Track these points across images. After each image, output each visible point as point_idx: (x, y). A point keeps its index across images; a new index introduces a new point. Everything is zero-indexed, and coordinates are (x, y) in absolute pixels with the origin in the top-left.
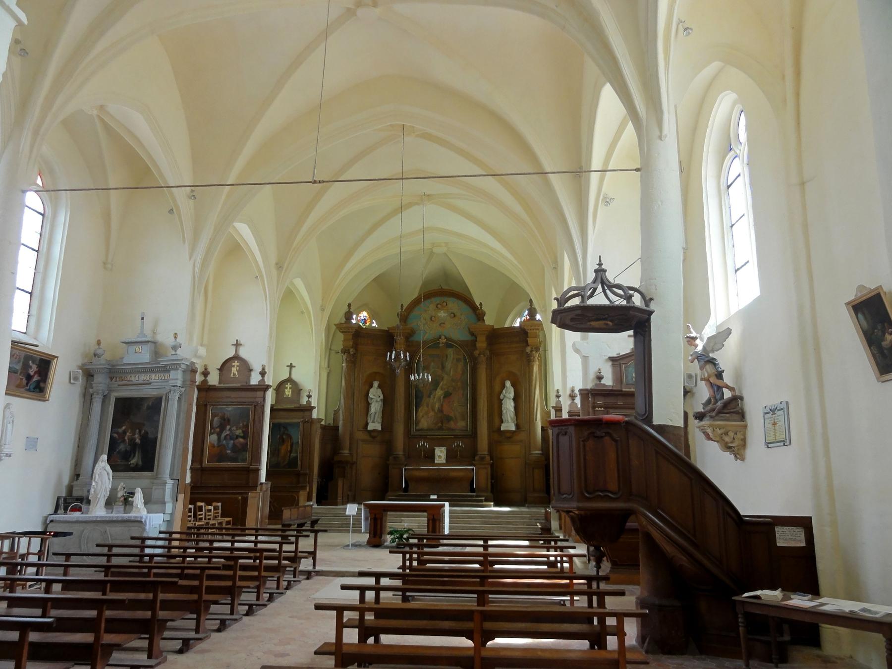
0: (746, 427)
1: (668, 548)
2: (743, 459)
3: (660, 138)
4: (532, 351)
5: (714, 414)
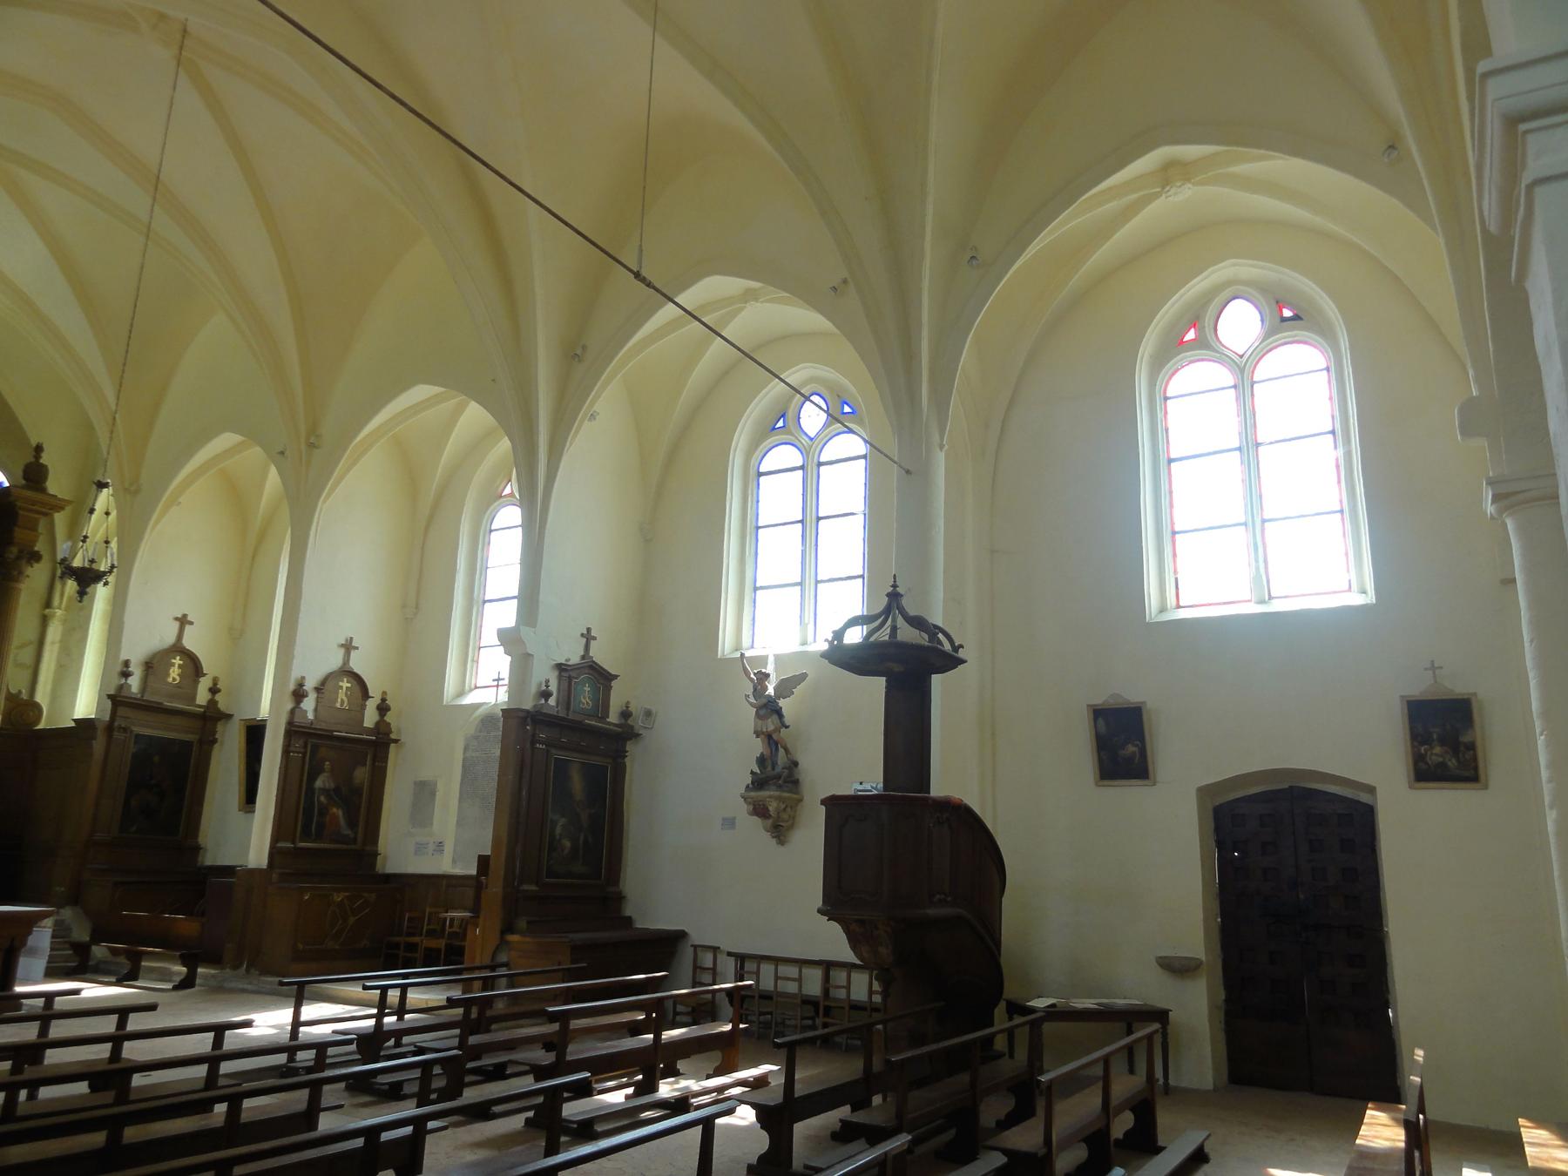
4: (18, 558)
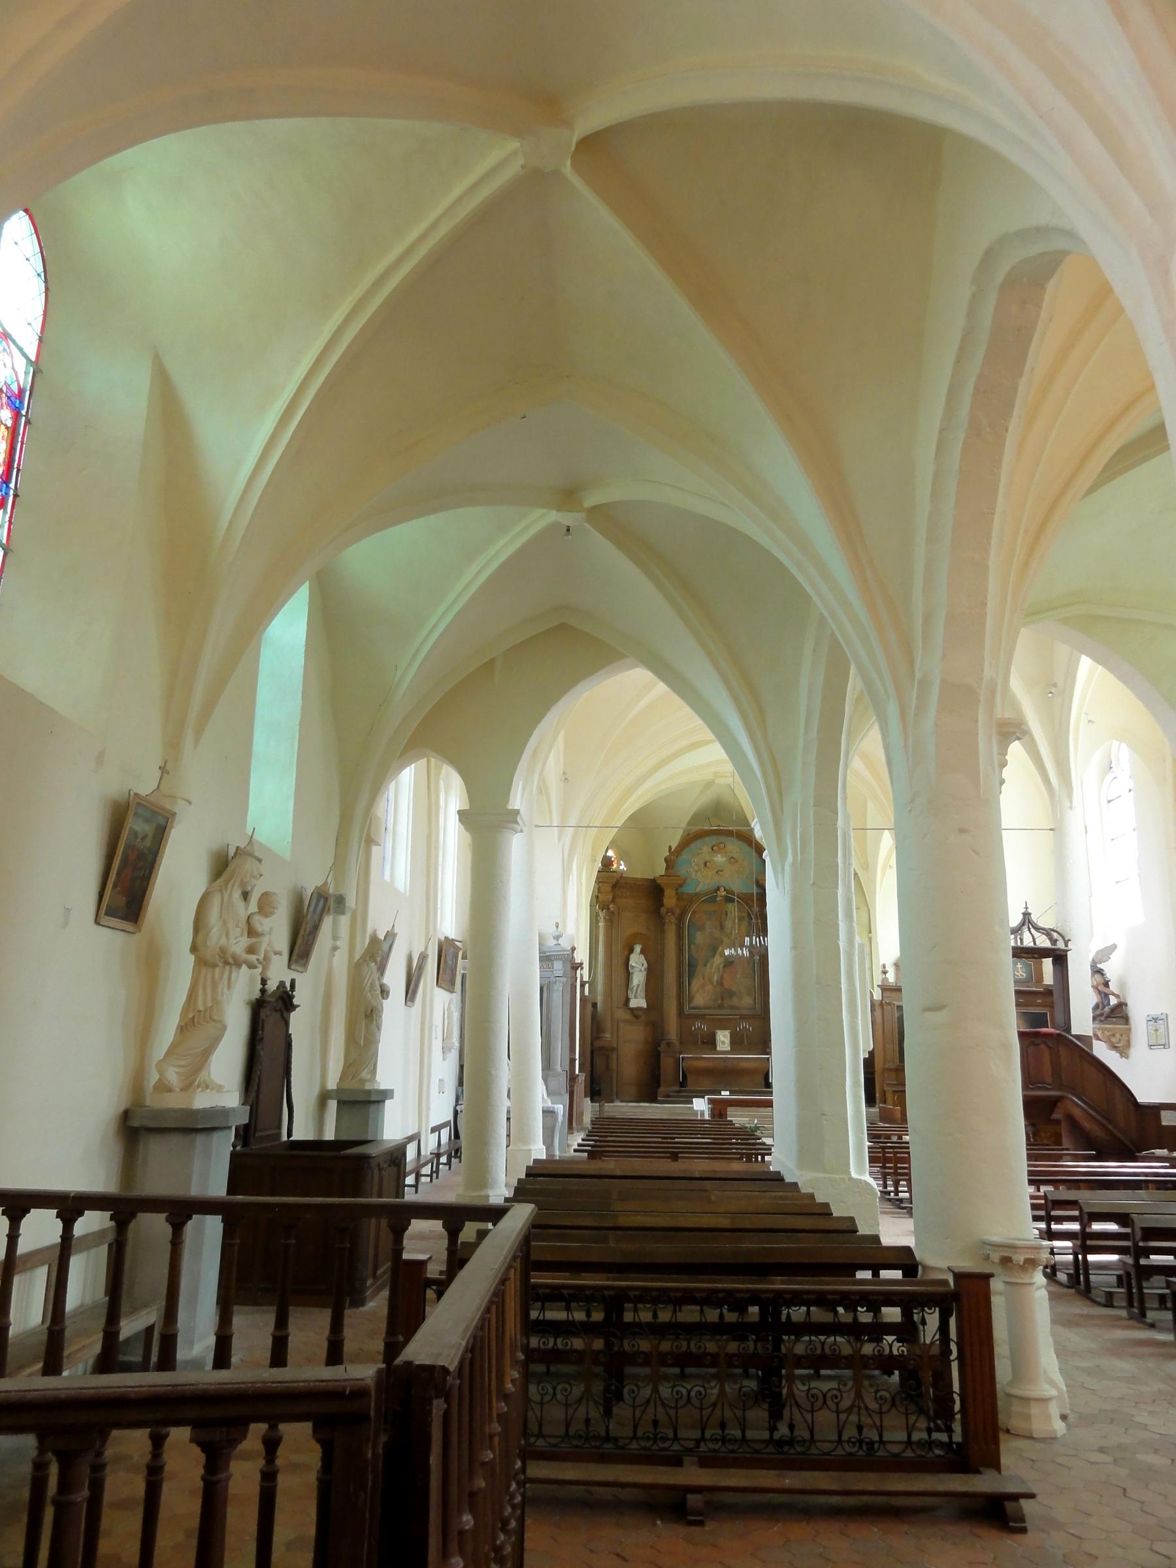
0: (1130, 1029)
1: (1087, 1125)
2: (1127, 1057)
3: (1071, 808)
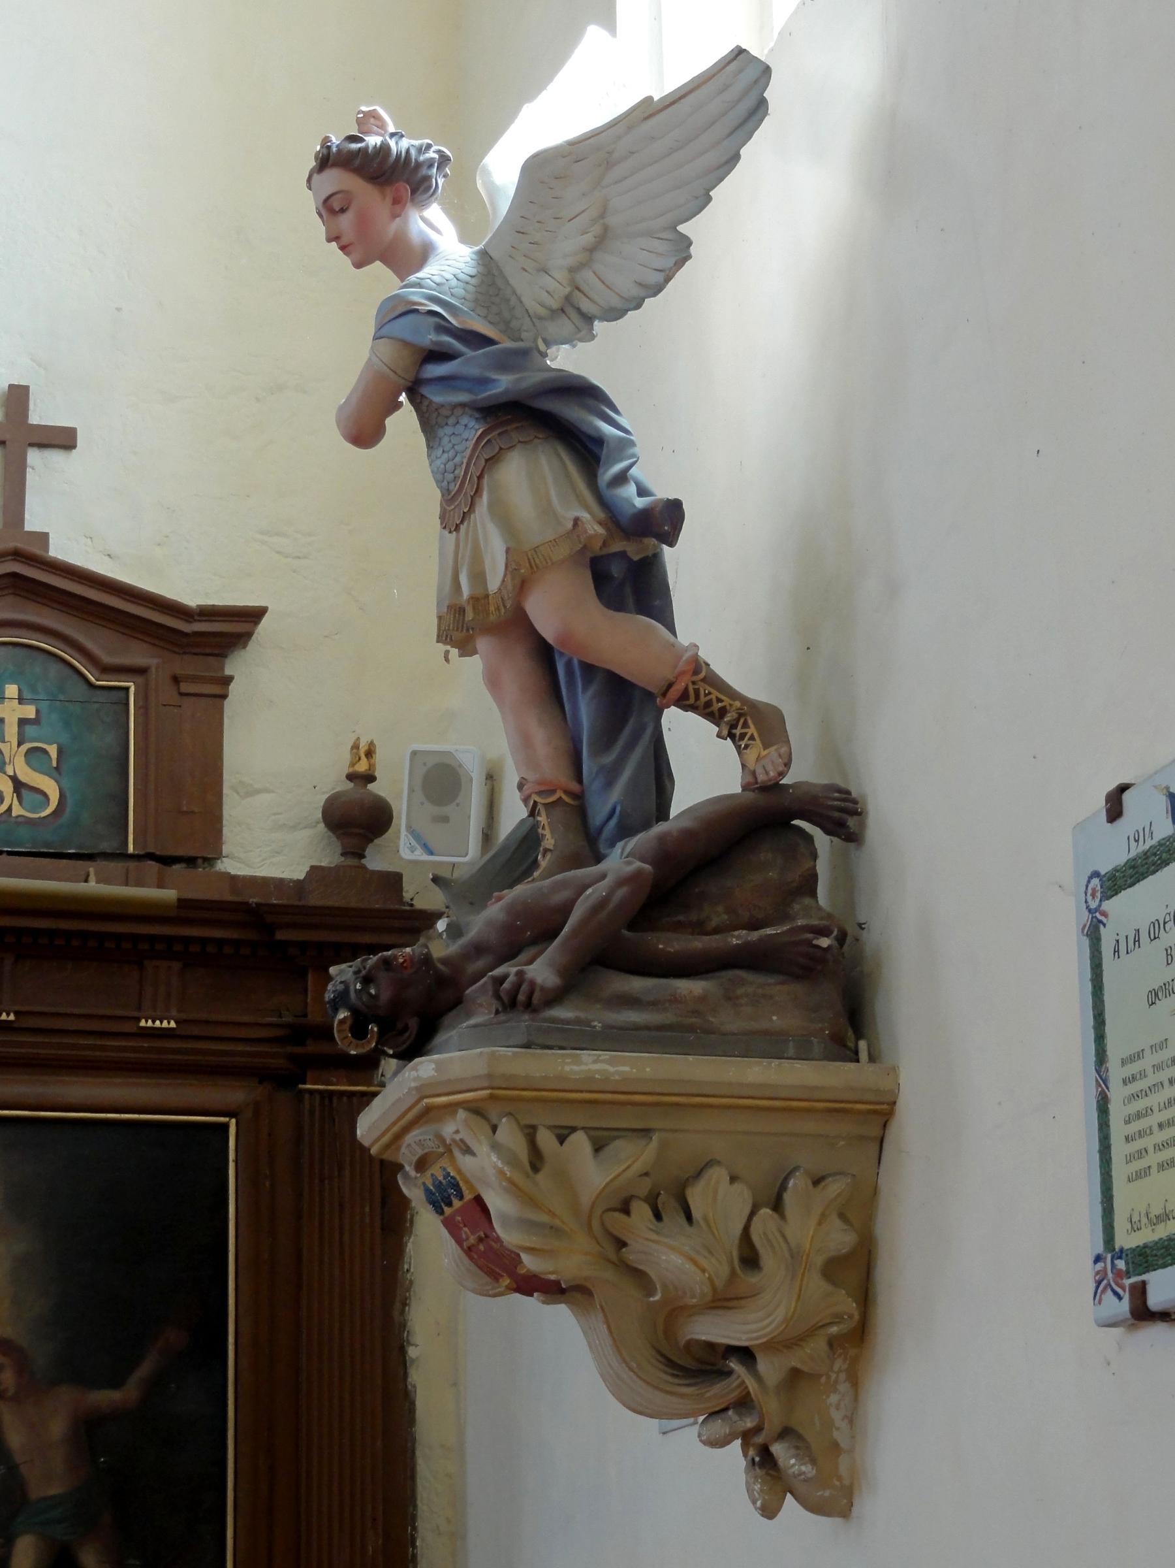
0: (877, 1117)
2: (835, 1499)
5: (542, 970)
